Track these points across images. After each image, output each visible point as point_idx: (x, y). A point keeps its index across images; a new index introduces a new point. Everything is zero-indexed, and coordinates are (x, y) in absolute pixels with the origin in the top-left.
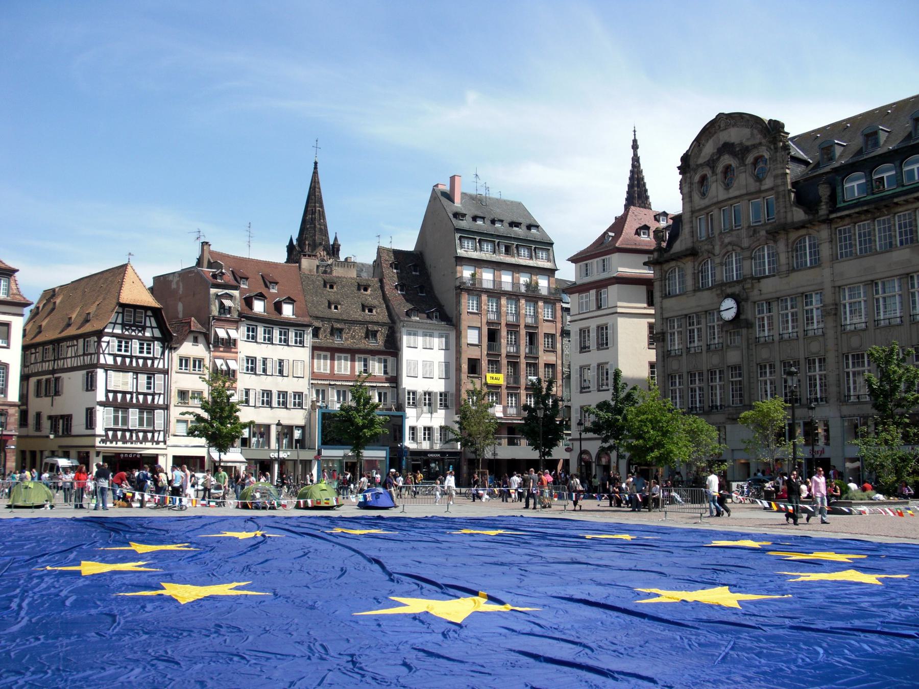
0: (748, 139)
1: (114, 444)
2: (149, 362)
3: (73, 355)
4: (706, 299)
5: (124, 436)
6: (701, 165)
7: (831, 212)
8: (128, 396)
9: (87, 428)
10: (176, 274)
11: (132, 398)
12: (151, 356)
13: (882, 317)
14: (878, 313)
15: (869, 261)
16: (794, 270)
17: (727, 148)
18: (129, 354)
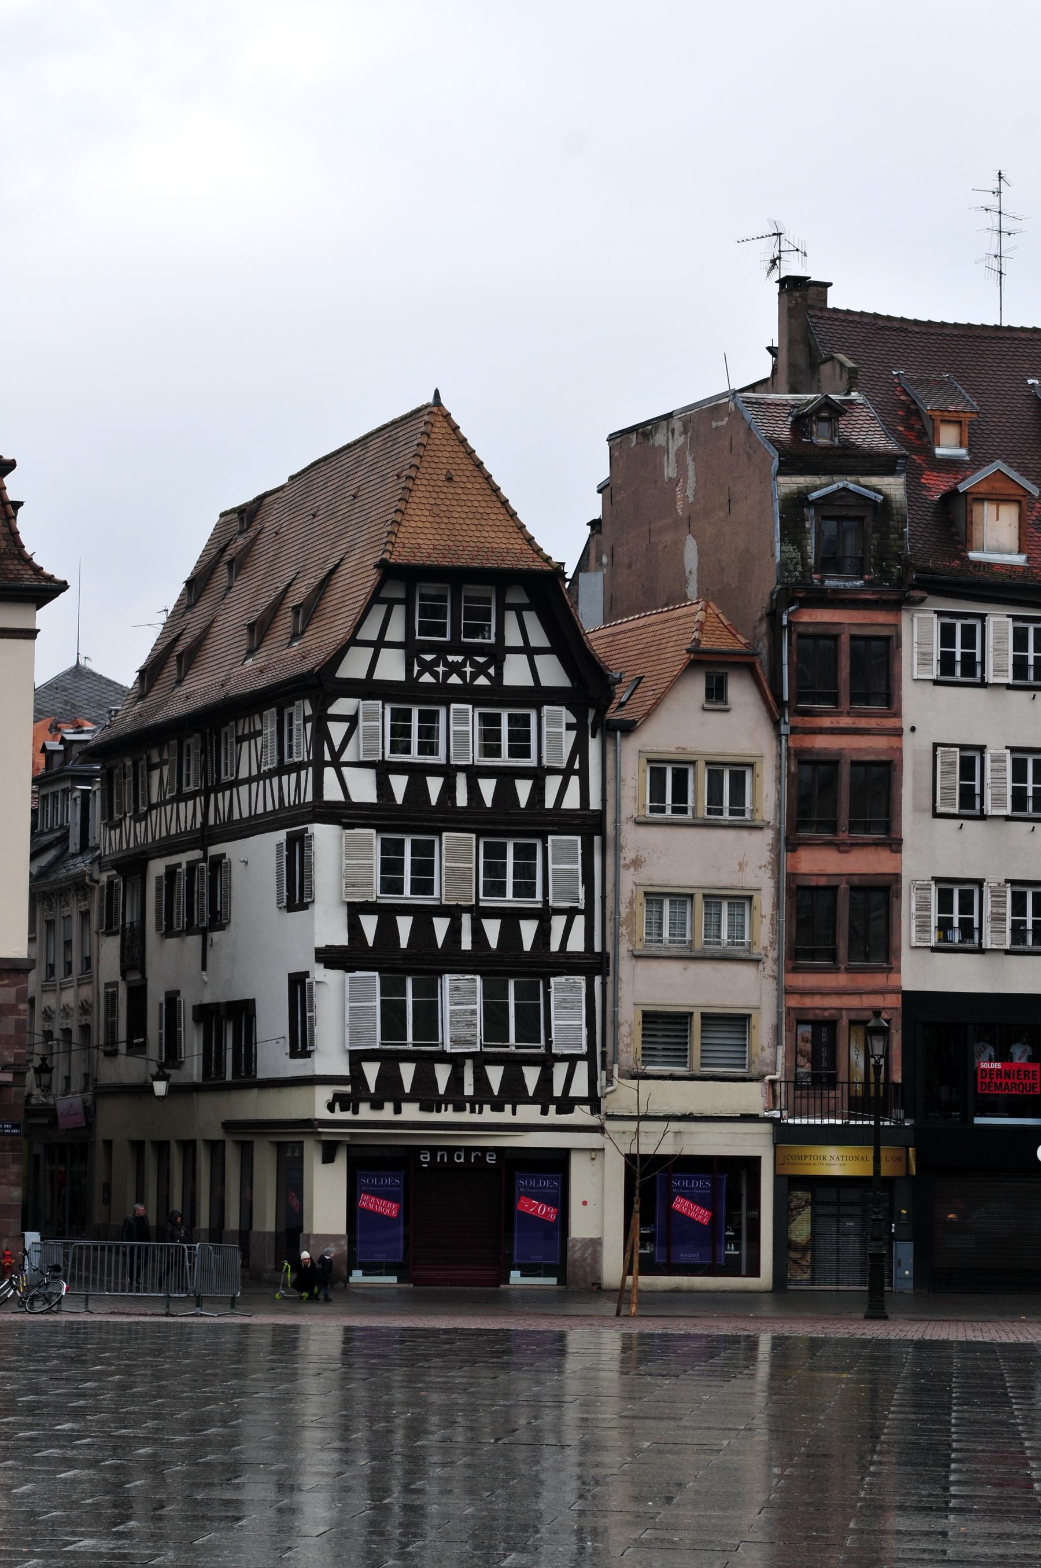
1: (387, 1113)
2: (523, 789)
3: (254, 772)
5: (425, 1080)
8: (441, 926)
9: (294, 1054)
10: (677, 424)
11: (454, 932)
12: (531, 762)
18: (440, 759)
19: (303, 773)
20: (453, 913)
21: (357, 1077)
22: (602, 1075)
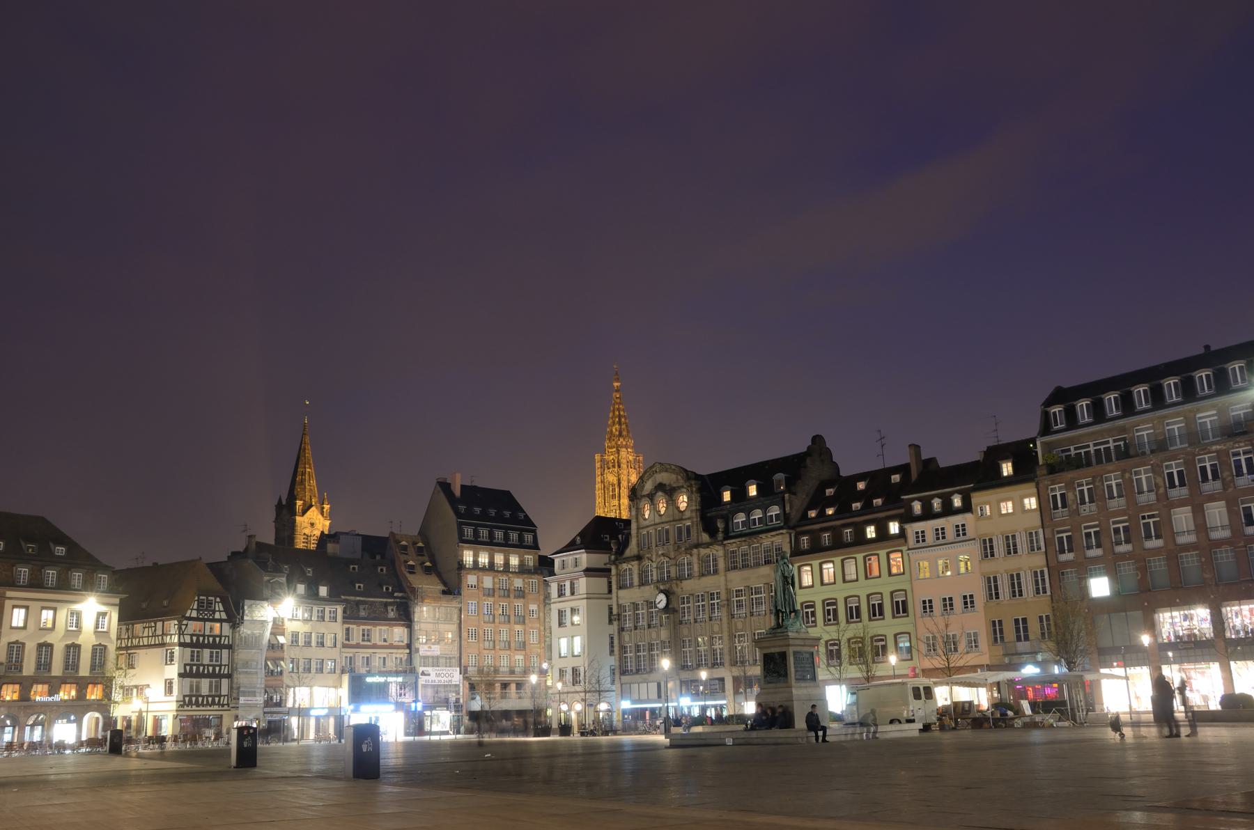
0: (674, 483)
3: (151, 634)
4: (648, 591)
5: (197, 700)
6: (644, 496)
7: (727, 537)
8: (201, 668)
11: (204, 669)
13: (755, 610)
14: (753, 608)
15: (746, 573)
16: (703, 575)
17: (660, 487)
19: (173, 636)
20: (204, 666)
21: (184, 701)
22: (230, 699)
